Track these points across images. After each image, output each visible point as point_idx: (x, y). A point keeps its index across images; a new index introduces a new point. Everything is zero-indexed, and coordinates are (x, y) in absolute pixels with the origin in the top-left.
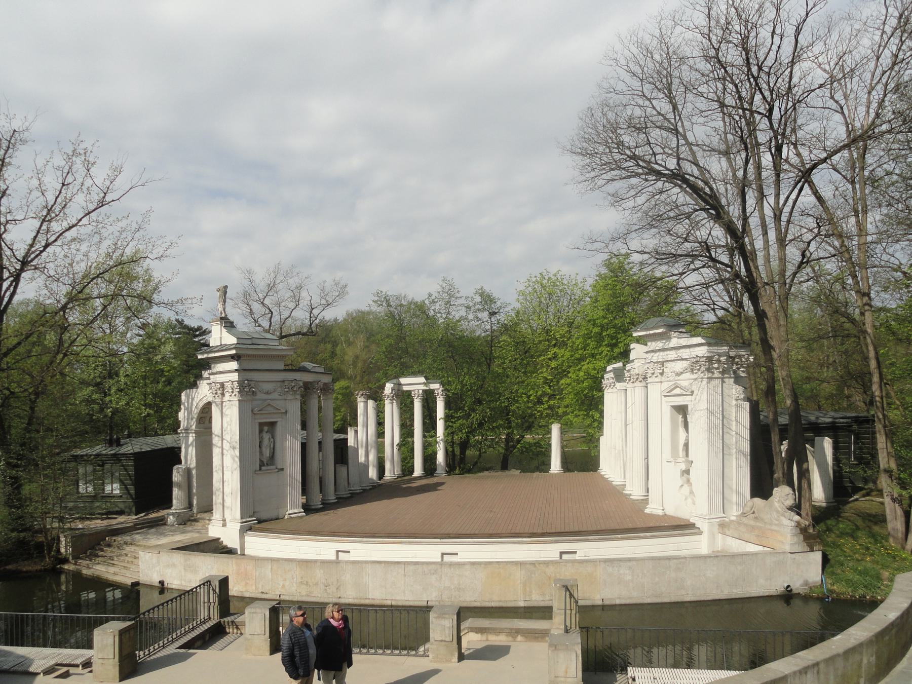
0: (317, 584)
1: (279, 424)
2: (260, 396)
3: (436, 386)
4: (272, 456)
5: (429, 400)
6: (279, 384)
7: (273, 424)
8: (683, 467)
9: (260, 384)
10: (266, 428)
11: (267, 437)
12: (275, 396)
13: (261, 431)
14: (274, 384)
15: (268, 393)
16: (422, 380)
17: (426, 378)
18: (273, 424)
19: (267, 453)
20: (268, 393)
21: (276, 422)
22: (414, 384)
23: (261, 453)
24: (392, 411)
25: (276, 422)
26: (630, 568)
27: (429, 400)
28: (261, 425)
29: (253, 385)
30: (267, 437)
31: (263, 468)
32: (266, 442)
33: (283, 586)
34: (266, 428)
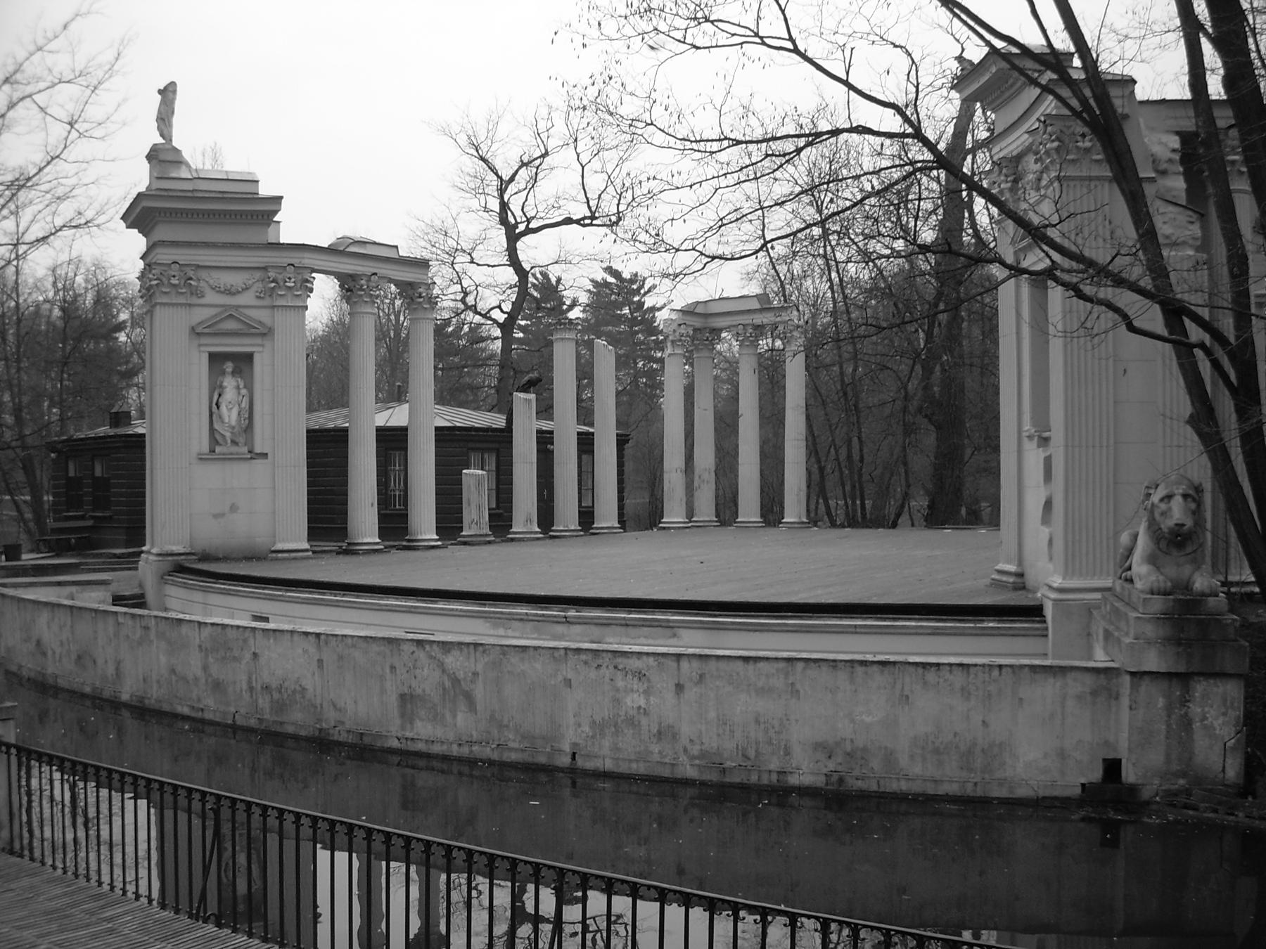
1: (257, 358)
2: (211, 298)
4: (248, 428)
6: (258, 275)
9: (215, 274)
11: (229, 383)
12: (247, 299)
15: (229, 292)
18: (244, 362)
19: (230, 416)
20: (229, 292)
21: (249, 358)
25: (249, 358)
26: (640, 675)
30: (229, 383)
31: (218, 449)
32: (230, 394)
34: (229, 367)
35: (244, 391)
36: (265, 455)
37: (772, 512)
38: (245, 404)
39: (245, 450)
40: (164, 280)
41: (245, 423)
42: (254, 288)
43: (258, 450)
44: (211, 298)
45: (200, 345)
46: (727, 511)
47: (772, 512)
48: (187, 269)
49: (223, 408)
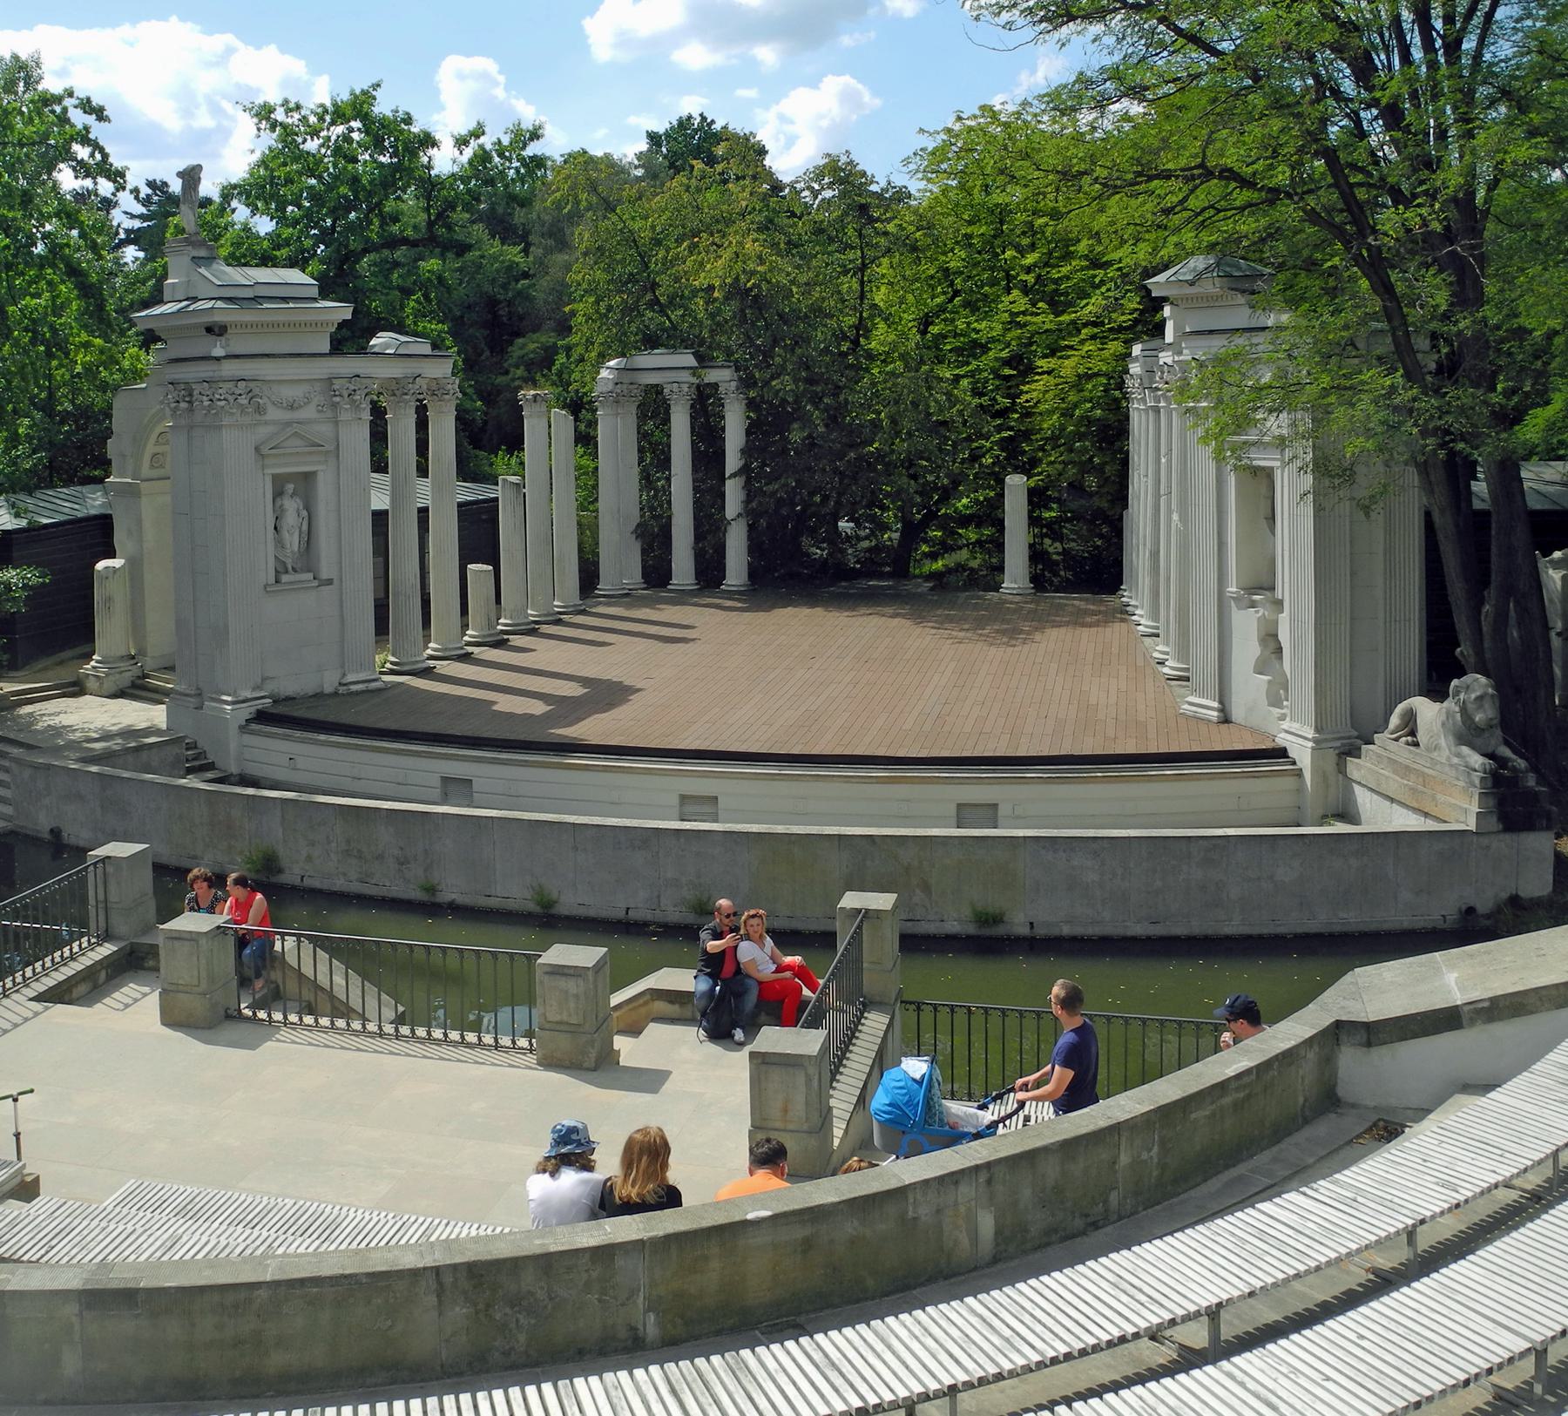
0: (380, 857)
1: (321, 477)
2: (273, 414)
3: (722, 376)
5: (705, 406)
7: (308, 478)
10: (290, 487)
11: (291, 506)
13: (278, 494)
14: (306, 388)
16: (688, 360)
17: (697, 356)
19: (293, 541)
20: (291, 407)
22: (669, 367)
23: (280, 543)
24: (616, 432)
25: (314, 474)
27: (705, 406)
28: (275, 477)
29: (256, 391)
31: (285, 578)
32: (291, 519)
33: (309, 858)
35: (305, 513)
36: (330, 582)
37: (710, 573)
38: (305, 527)
39: (310, 576)
40: (231, 399)
41: (304, 546)
42: (315, 402)
43: (324, 575)
44: (273, 414)
45: (263, 468)
46: (657, 575)
47: (710, 573)
48: (252, 385)
49: (286, 535)
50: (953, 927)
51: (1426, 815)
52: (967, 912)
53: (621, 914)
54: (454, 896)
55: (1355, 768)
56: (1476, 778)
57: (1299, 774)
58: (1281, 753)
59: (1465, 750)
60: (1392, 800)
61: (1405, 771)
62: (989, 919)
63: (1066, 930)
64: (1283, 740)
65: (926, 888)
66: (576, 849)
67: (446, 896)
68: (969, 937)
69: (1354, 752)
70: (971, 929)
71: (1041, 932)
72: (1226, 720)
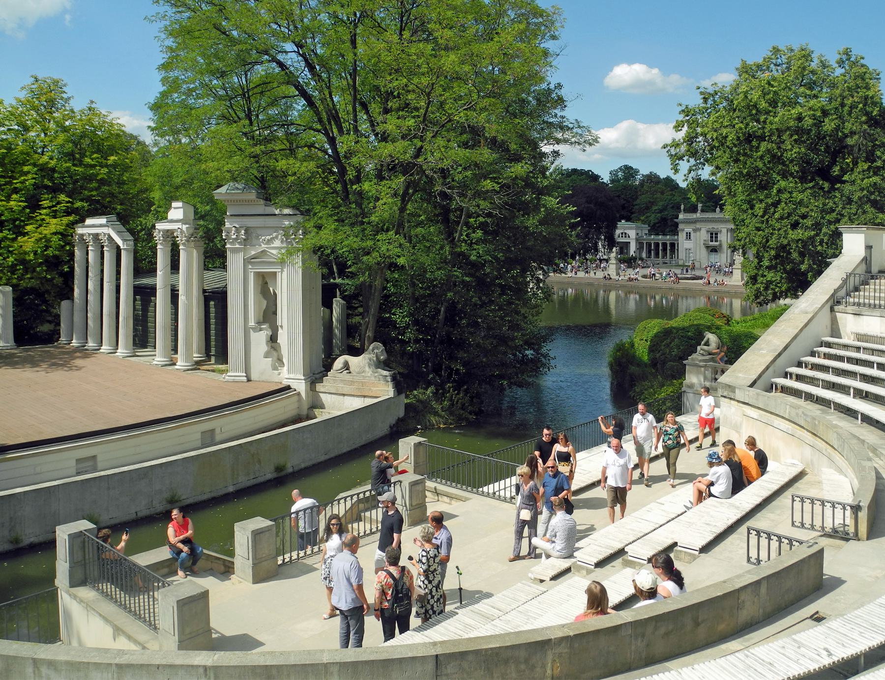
8: (270, 333)
50: (269, 476)
51: (365, 397)
52: (272, 468)
53: (133, 516)
54: (32, 540)
55: (319, 387)
56: (389, 379)
57: (299, 394)
58: (288, 388)
59: (379, 370)
60: (344, 395)
61: (352, 383)
62: (279, 469)
63: (303, 466)
64: (286, 383)
65: (259, 462)
66: (109, 488)
67: (26, 541)
68: (276, 479)
69: (321, 380)
70: (275, 475)
71: (296, 469)
72: (249, 380)
